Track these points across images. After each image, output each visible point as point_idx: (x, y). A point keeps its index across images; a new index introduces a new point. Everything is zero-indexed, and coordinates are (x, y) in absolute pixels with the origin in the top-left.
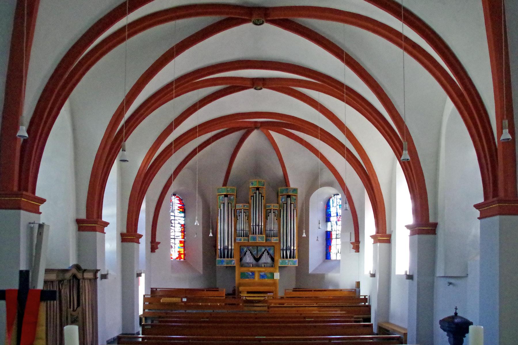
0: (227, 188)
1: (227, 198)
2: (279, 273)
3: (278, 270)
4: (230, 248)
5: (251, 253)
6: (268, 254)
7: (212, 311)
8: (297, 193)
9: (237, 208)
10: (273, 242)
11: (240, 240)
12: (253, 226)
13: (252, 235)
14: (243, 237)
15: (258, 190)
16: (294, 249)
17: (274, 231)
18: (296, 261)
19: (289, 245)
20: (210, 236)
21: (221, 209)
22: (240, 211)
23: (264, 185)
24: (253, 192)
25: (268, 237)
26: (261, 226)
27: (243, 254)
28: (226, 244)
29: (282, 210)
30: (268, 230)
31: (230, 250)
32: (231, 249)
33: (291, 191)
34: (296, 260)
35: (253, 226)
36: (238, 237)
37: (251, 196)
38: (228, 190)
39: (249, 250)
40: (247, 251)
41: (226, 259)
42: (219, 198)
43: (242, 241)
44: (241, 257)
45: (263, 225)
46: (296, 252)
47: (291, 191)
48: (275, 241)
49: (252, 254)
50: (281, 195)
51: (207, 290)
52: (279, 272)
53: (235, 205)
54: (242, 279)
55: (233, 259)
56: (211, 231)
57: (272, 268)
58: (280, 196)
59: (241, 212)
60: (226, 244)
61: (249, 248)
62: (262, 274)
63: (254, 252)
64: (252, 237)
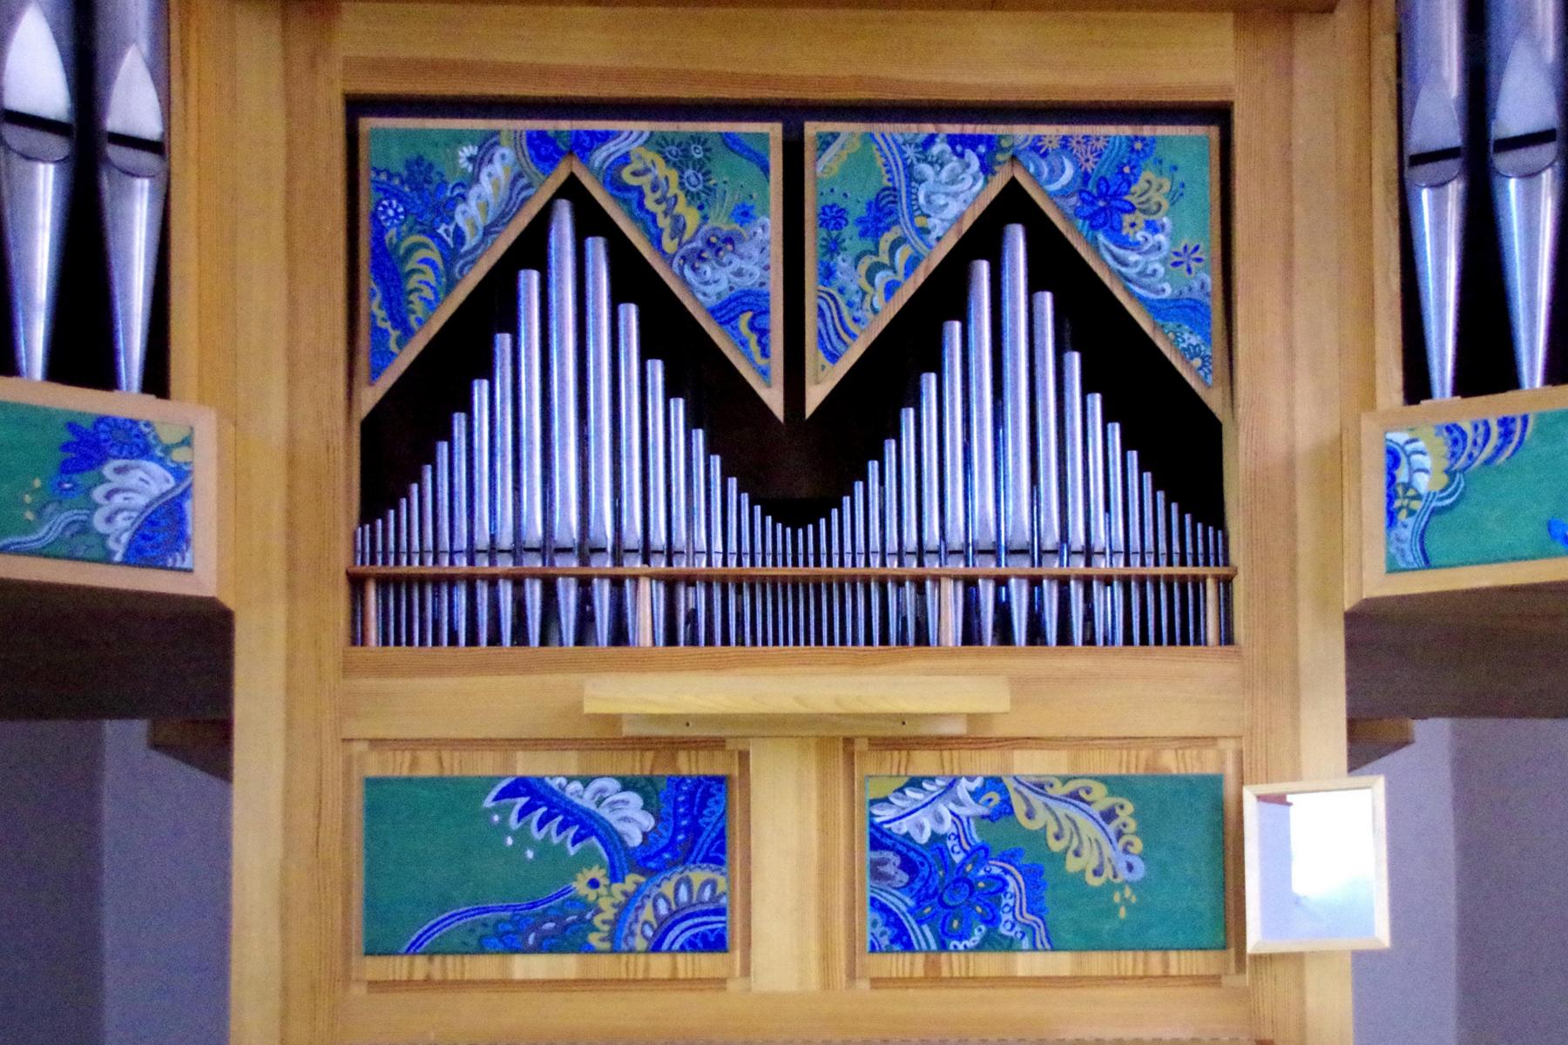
39: (590, 220)
54: (397, 967)
61: (583, 145)
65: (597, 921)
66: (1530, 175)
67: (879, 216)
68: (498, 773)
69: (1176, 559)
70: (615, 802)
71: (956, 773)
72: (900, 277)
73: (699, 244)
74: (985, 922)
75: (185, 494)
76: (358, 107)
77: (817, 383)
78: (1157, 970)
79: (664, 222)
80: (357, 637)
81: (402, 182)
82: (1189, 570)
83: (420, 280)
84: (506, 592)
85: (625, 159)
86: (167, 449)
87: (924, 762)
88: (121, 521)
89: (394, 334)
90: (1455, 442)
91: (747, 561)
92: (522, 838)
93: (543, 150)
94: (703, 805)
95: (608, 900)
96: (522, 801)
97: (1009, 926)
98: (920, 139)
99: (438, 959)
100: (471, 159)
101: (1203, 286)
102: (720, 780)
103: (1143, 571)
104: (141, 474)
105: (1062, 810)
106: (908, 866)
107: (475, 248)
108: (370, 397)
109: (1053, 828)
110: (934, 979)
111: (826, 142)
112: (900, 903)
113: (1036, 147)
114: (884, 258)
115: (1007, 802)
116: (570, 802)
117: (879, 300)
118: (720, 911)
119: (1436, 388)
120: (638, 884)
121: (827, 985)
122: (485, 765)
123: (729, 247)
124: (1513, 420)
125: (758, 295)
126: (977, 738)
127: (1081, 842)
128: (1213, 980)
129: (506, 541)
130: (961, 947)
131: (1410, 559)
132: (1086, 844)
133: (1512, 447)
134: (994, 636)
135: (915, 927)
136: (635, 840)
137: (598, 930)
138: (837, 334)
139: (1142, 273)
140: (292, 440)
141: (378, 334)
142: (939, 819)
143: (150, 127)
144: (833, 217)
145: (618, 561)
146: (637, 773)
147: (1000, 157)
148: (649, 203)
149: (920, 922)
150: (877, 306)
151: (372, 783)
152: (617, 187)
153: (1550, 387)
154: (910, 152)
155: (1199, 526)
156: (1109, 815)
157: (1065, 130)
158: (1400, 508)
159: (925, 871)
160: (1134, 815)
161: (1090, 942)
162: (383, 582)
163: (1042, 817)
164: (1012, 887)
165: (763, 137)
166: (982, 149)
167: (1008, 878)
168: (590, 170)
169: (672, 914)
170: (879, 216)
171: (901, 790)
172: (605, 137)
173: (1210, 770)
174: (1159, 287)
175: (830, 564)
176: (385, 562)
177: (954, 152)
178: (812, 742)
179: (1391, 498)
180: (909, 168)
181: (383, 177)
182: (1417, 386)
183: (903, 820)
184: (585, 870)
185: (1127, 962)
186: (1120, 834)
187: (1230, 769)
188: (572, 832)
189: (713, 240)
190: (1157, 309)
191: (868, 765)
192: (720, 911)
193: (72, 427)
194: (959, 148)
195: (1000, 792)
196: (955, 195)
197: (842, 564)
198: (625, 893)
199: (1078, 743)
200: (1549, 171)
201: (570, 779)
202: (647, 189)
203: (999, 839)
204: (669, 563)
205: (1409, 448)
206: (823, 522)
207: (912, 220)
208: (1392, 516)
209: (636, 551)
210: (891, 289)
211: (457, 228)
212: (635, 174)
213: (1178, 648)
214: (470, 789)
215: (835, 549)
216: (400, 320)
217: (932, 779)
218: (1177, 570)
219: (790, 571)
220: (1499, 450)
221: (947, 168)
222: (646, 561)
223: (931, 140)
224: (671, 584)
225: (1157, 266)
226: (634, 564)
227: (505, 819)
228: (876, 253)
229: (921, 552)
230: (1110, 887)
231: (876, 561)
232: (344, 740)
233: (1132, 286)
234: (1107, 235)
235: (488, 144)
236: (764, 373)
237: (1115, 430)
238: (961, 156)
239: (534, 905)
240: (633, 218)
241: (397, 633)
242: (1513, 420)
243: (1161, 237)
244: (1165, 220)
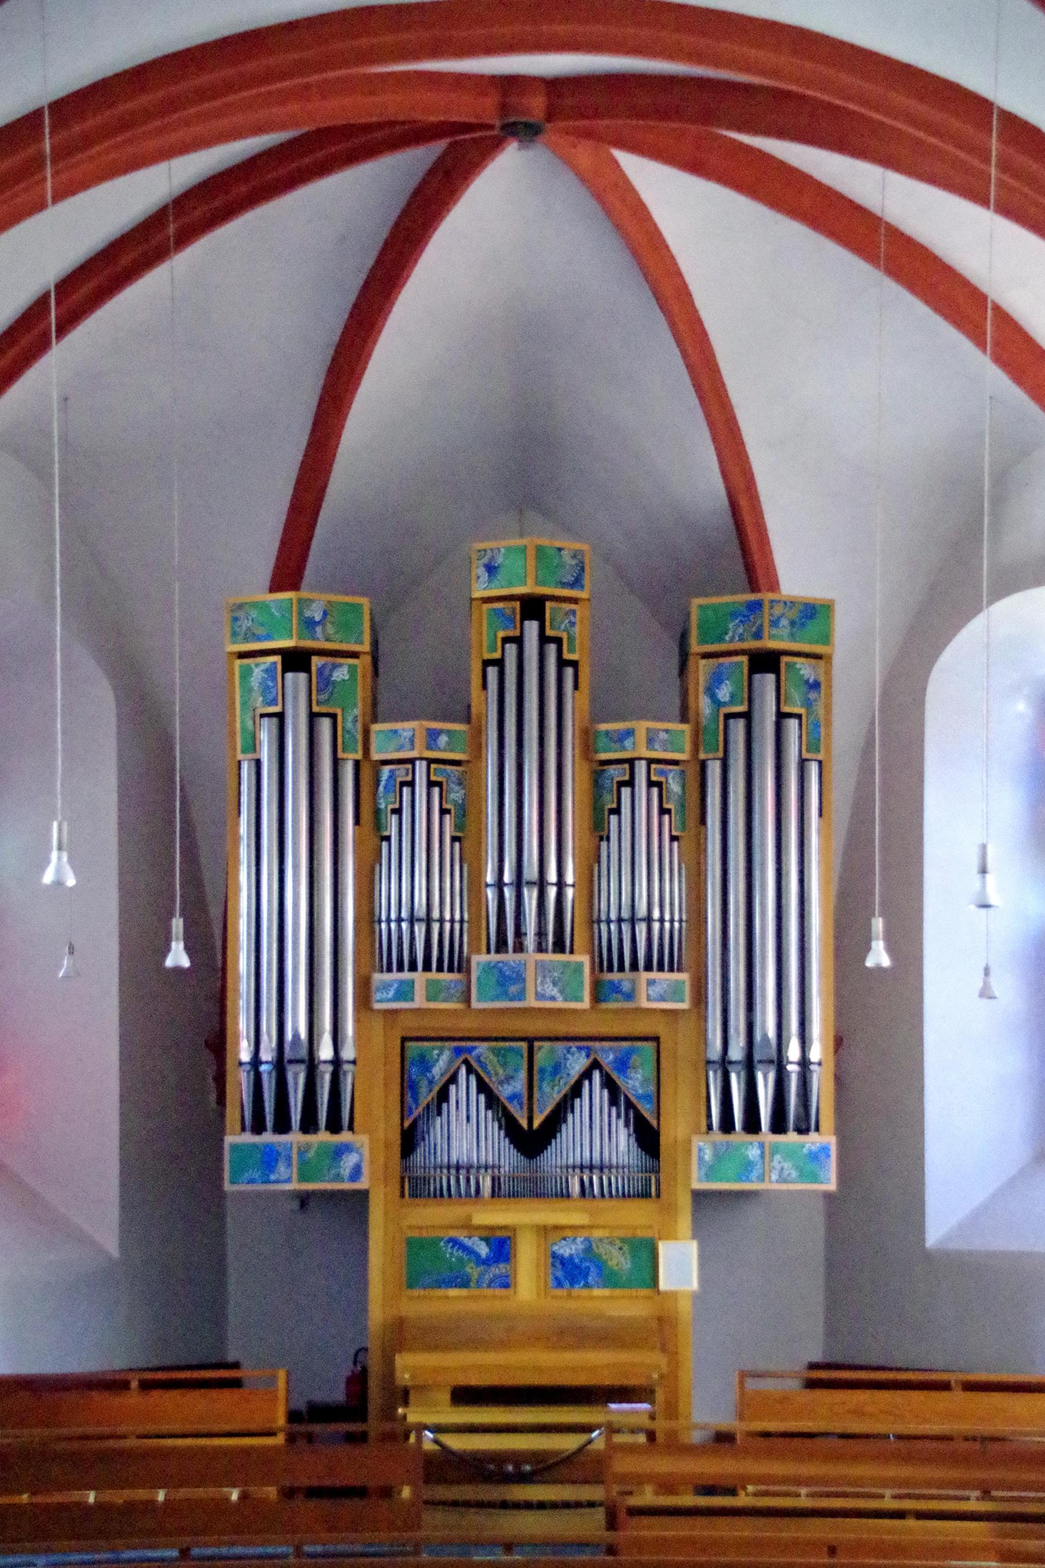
0: (300, 601)
1: (302, 676)
2: (693, 1247)
3: (685, 1222)
4: (325, 1052)
5: (483, 1087)
6: (614, 1101)
7: (175, 1553)
8: (826, 638)
9: (376, 756)
10: (645, 1004)
11: (405, 992)
12: (500, 885)
13: (494, 957)
14: (427, 967)
15: (531, 618)
16: (804, 1063)
17: (656, 926)
18: (825, 1149)
19: (772, 1033)
20: (169, 962)
21: (258, 763)
22: (402, 773)
23: (577, 583)
24: (501, 634)
25: (610, 969)
26: (561, 884)
27: (427, 1096)
28: (298, 1022)
29: (714, 770)
30: (613, 916)
31: (322, 1068)
32: (337, 1062)
33: (784, 622)
34: (824, 1139)
35: (500, 885)
36: (389, 970)
37: (487, 663)
38: (308, 614)
39: (470, 1070)
40: (453, 1079)
41: (295, 1137)
42: (246, 673)
43: (419, 1001)
44: (406, 1124)
45: (570, 878)
46: (821, 1083)
47: (784, 622)
48: (662, 999)
49: (492, 1101)
50: (707, 656)
51: (146, 1386)
52: (694, 1237)
53: (366, 733)
54: (416, 1292)
55: (345, 1136)
56: (178, 924)
57: (642, 1203)
58: (703, 662)
59: (411, 784)
60: (298, 1022)
61: (470, 1050)
62: (566, 1250)
63: (509, 1079)
64: (489, 968)
73: (503, 1078)
79: (492, 1072)
80: (402, 1195)
83: (423, 1090)
87: (568, 1233)
92: (451, 1254)
93: (458, 1051)
96: (451, 1244)
102: (509, 1238)
105: (609, 1247)
106: (563, 1264)
109: (604, 1252)
110: (569, 1295)
111: (540, 1048)
112: (560, 1274)
126: (583, 1227)
139: (633, 1086)
141: (411, 1110)
144: (542, 1071)
156: (620, 1249)
161: (615, 1285)
172: (475, 1048)
185: (627, 1292)
187: (656, 1236)
190: (639, 1097)
199: (612, 1228)
210: (559, 1092)
216: (416, 1100)
223: (571, 1047)
227: (447, 1249)
235: (441, 1050)
241: (414, 1195)
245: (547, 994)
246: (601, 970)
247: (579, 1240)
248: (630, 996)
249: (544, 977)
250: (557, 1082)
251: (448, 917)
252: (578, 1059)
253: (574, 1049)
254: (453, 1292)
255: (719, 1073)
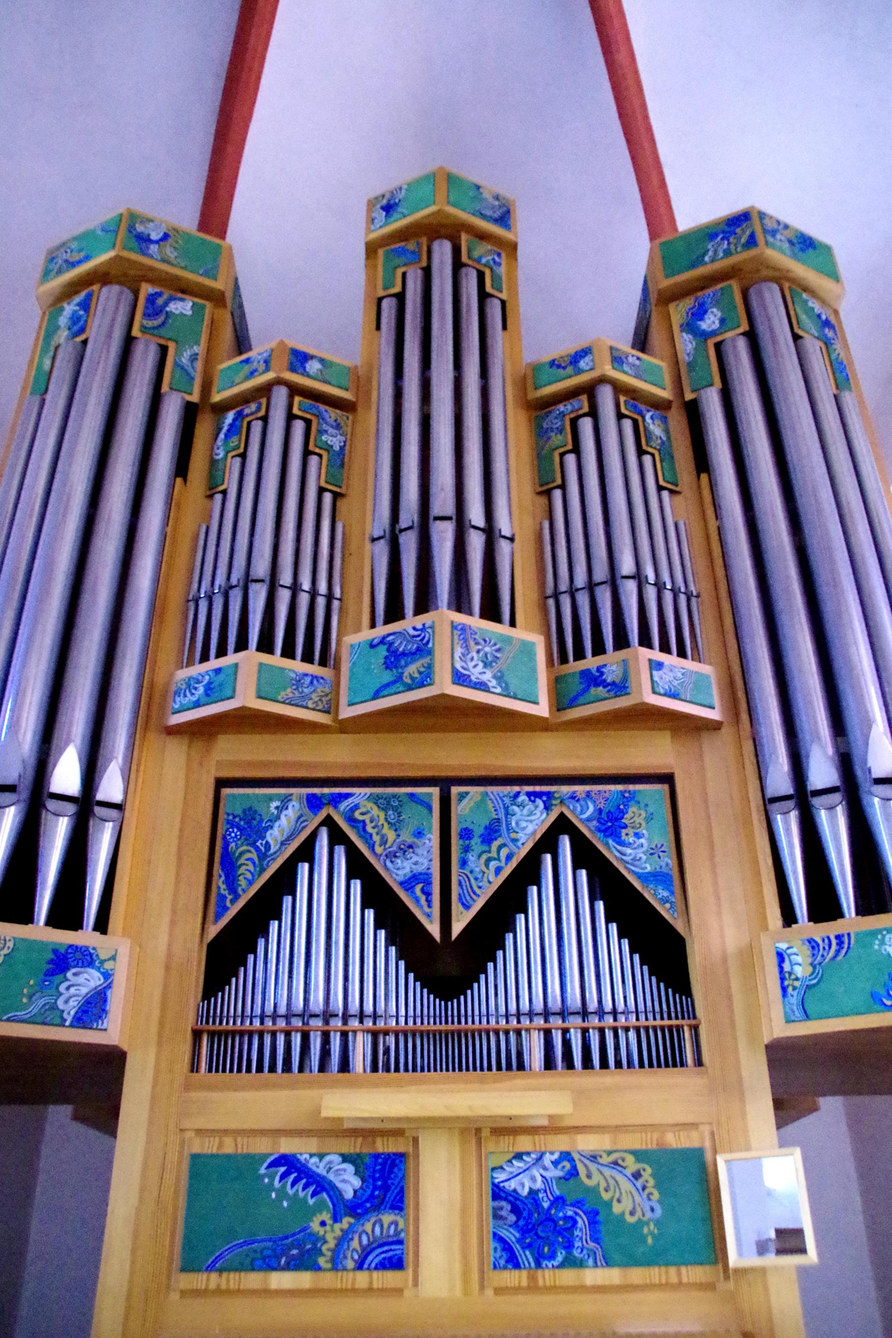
39: (337, 837)
40: (306, 852)
61: (336, 800)
65: (324, 1248)
66: (831, 808)
67: (490, 834)
68: (269, 1151)
69: (665, 1015)
70: (338, 1170)
71: (543, 1149)
72: (503, 864)
73: (394, 848)
74: (565, 1248)
75: (109, 986)
76: (221, 783)
77: (458, 921)
78: (674, 1279)
79: (376, 838)
80: (194, 1067)
81: (241, 819)
82: (674, 1022)
83: (245, 870)
84: (281, 1039)
85: (356, 807)
86: (102, 962)
87: (524, 1143)
88: (73, 1003)
89: (230, 897)
90: (813, 948)
91: (419, 1021)
93: (314, 803)
94: (391, 1172)
95: (332, 1234)
96: (283, 1169)
97: (579, 1250)
98: (512, 794)
99: (225, 1275)
100: (277, 808)
101: (667, 864)
102: (402, 1156)
103: (647, 1023)
104: (86, 976)
105: (607, 1172)
106: (515, 1210)
107: (275, 853)
108: (213, 931)
110: (533, 1288)
111: (462, 796)
112: (511, 1235)
113: (573, 797)
114: (494, 854)
115: (574, 1167)
116: (310, 1169)
117: (492, 877)
118: (400, 1242)
119: (800, 921)
120: (350, 1225)
121: (466, 1292)
122: (262, 1146)
123: (411, 850)
124: (843, 936)
125: (427, 874)
126: (554, 1127)
127: (621, 1193)
128: (710, 1287)
129: (282, 1010)
130: (550, 1266)
131: (797, 1013)
132: (624, 1195)
133: (844, 951)
134: (562, 1062)
135: (521, 1252)
136: (349, 1194)
137: (324, 1255)
138: (470, 895)
139: (634, 859)
140: (169, 955)
141: (222, 898)
142: (533, 1179)
143: (117, 797)
144: (466, 834)
145: (345, 1023)
146: (352, 1151)
147: (554, 802)
148: (369, 829)
149: (523, 1248)
150: (491, 880)
151: (195, 1157)
152: (351, 820)
153: (860, 917)
154: (507, 800)
155: (677, 996)
156: (637, 1175)
157: (588, 788)
158: (788, 986)
159: (525, 1214)
160: (653, 1175)
161: (631, 1261)
162: (212, 1034)
163: (597, 1178)
164: (580, 1223)
165: (430, 795)
166: (545, 798)
167: (578, 1218)
168: (338, 812)
169: (370, 1244)
170: (490, 834)
171: (510, 1161)
172: (347, 796)
173: (696, 1144)
174: (644, 866)
175: (466, 1023)
176: (214, 1023)
177: (530, 800)
178: (457, 1133)
179: (782, 979)
180: (506, 808)
181: (231, 817)
182: (789, 917)
183: (512, 1181)
184: (318, 1215)
185: (654, 1274)
186: (644, 1188)
187: (708, 1144)
188: (312, 1189)
189: (402, 846)
190: (644, 878)
191: (490, 1145)
192: (400, 1242)
193: (55, 951)
194: (532, 798)
195: (569, 1161)
196: (531, 821)
197: (473, 1022)
198: (342, 1230)
200: (840, 806)
201: (311, 1155)
202: (368, 822)
203: (571, 1192)
204: (375, 1023)
205: (789, 951)
206: (462, 998)
207: (508, 834)
208: (784, 989)
209: (355, 1016)
210: (498, 870)
211: (267, 842)
212: (362, 814)
213: (671, 1069)
214: (254, 1160)
215: (470, 1012)
217: (528, 1154)
218: (666, 1022)
219: (443, 1027)
220: (838, 952)
221: (527, 808)
222: (361, 1022)
223: (517, 794)
224: (375, 1034)
225: (642, 855)
226: (354, 1023)
228: (489, 852)
229: (518, 1015)
230: (640, 1223)
231: (493, 1021)
232: (181, 1130)
233: (629, 866)
234: (614, 841)
235: (285, 801)
236: (429, 916)
237: (625, 943)
238: (534, 802)
239: (287, 1238)
240: (361, 836)
242: (843, 936)
243: (642, 841)
244: (644, 832)
245: (473, 678)
246: (564, 660)
247: (548, 1159)
248: (620, 688)
249: (467, 648)
250: (494, 854)
251: (306, 585)
252: (531, 814)
253: (523, 798)
254: (281, 1280)
255: (794, 816)
